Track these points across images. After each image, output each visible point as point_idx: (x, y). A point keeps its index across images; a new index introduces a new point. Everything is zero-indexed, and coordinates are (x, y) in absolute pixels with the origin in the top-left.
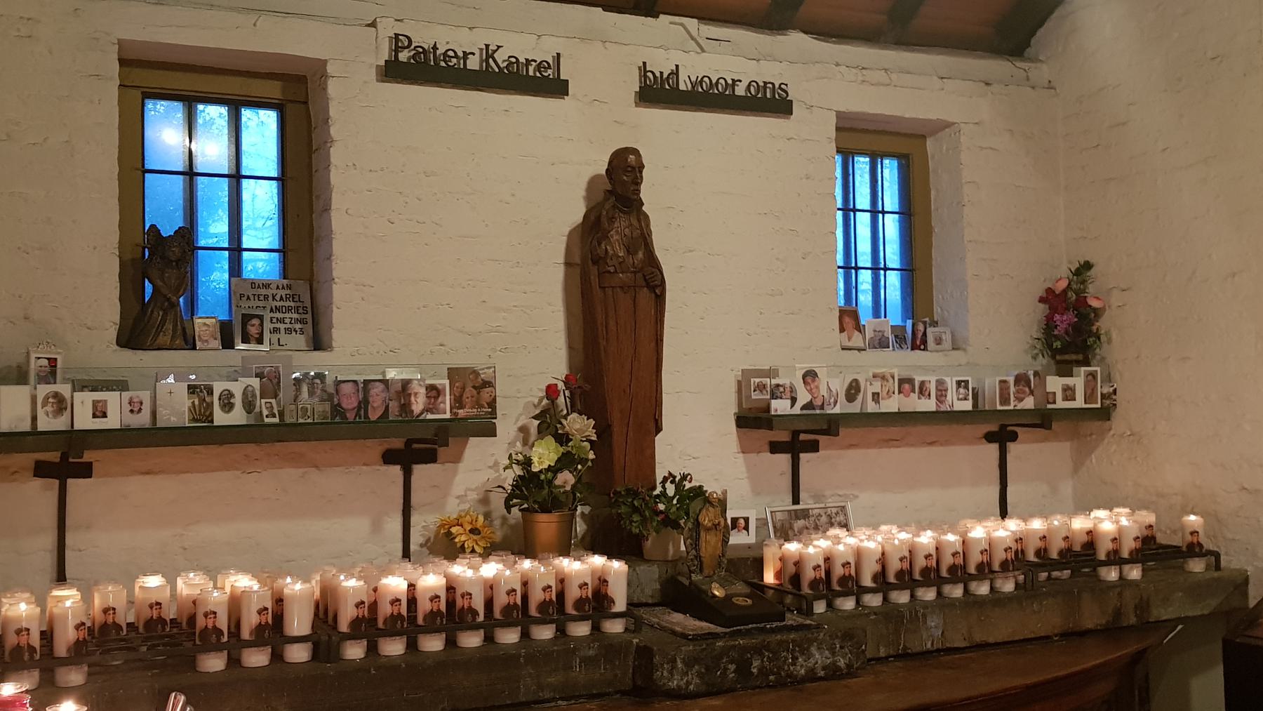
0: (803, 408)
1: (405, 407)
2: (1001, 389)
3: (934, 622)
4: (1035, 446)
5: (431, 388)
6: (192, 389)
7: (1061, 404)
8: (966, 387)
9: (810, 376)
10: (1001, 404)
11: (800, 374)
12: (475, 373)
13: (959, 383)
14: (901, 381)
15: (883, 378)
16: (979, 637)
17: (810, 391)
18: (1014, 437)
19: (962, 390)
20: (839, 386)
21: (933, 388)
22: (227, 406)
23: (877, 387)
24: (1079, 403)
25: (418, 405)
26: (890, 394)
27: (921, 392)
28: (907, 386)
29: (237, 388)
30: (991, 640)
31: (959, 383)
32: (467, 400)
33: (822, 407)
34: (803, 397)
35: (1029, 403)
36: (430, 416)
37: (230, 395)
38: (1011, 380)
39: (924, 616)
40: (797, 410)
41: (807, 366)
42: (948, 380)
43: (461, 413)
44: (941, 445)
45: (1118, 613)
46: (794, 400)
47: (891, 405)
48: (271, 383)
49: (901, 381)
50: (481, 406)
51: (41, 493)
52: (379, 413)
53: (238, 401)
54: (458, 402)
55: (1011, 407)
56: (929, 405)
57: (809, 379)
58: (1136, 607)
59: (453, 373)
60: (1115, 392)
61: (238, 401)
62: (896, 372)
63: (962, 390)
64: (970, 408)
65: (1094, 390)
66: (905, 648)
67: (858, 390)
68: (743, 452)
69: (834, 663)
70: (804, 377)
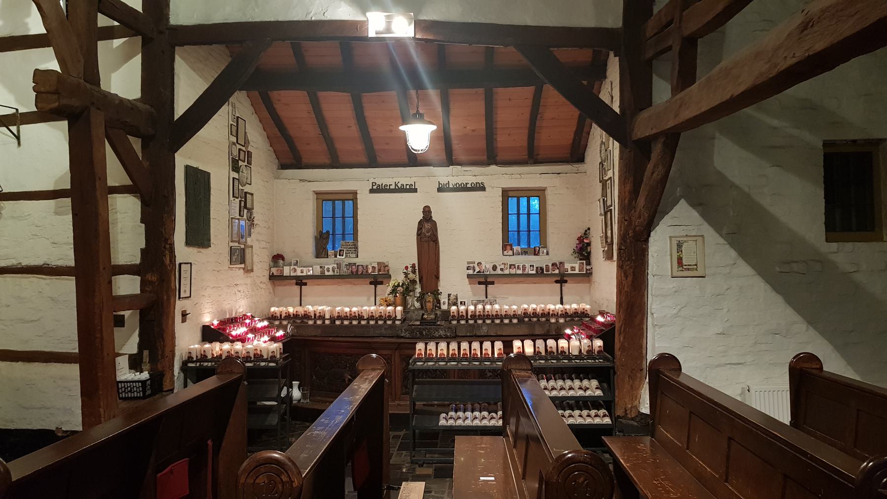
0: (477, 273)
1: (367, 271)
2: (546, 267)
3: (484, 328)
4: (575, 285)
5: (373, 267)
6: (321, 267)
7: (570, 272)
8: (533, 267)
9: (479, 264)
10: (546, 272)
11: (476, 263)
12: (384, 263)
13: (531, 266)
14: (511, 265)
15: (505, 264)
16: (499, 333)
17: (479, 268)
18: (566, 282)
19: (531, 268)
20: (489, 266)
21: (521, 267)
22: (328, 271)
23: (502, 267)
24: (577, 271)
25: (370, 272)
26: (507, 269)
27: (518, 268)
28: (513, 267)
29: (331, 267)
30: (504, 334)
31: (531, 266)
32: (382, 270)
33: (483, 272)
34: (477, 269)
35: (557, 271)
36: (373, 274)
37: (329, 268)
38: (550, 265)
39: (482, 326)
40: (475, 273)
41: (479, 261)
42: (527, 265)
43: (380, 273)
44: (539, 283)
45: (548, 331)
46: (474, 270)
47: (507, 272)
48: (339, 266)
49: (511, 265)
50: (385, 271)
51: (297, 288)
52: (361, 273)
53: (331, 270)
54: (379, 270)
55: (550, 273)
56: (520, 272)
57: (479, 265)
58: (555, 330)
59: (379, 263)
60: (592, 268)
61: (331, 270)
62: (508, 262)
63: (531, 268)
64: (534, 273)
65: (583, 268)
66: (475, 334)
67: (496, 267)
68: (470, 284)
69: (446, 334)
70: (478, 264)
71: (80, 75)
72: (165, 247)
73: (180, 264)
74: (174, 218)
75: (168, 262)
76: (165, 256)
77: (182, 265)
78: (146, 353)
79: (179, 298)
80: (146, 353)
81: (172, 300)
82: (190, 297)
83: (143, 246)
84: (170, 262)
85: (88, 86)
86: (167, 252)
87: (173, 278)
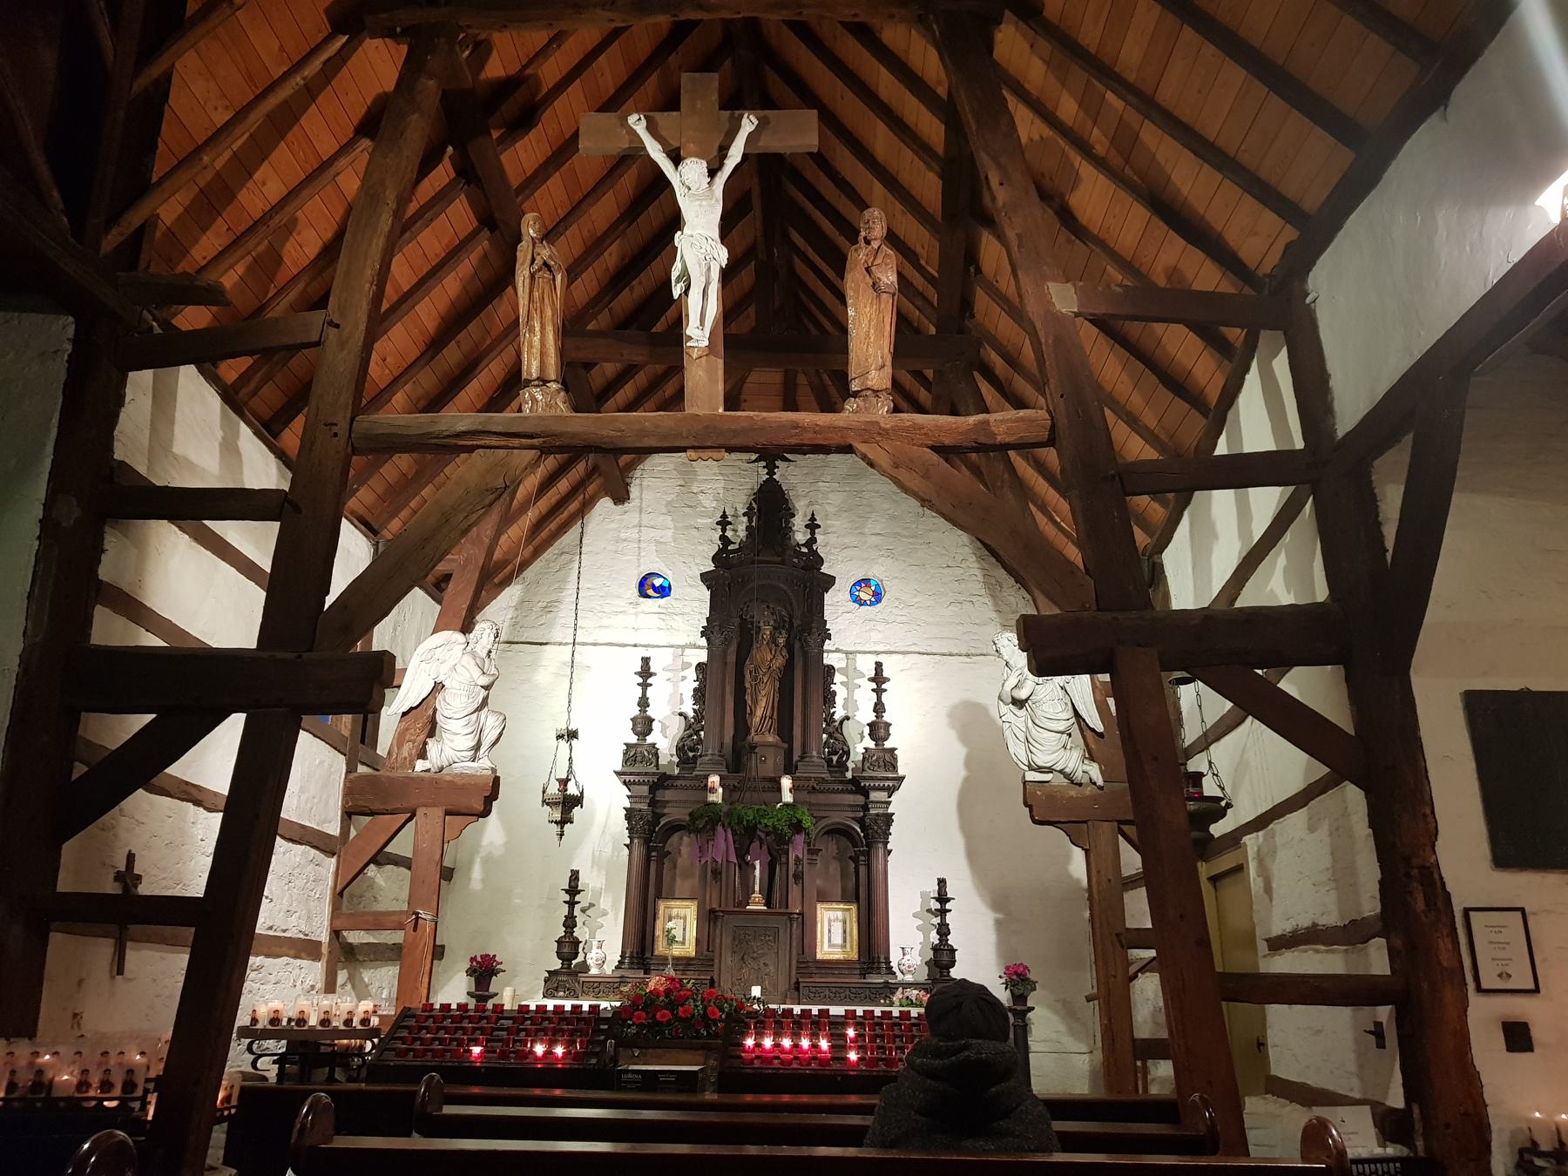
71: (1088, 606)
72: (1407, 875)
73: (1466, 912)
74: (1428, 811)
75: (1420, 904)
76: (1411, 893)
77: (1472, 914)
78: (1416, 1110)
79: (1479, 989)
80: (1416, 1110)
81: (1449, 995)
82: (1537, 990)
83: (1379, 876)
84: (1427, 905)
85: (1108, 616)
86: (1415, 884)
87: (1444, 944)
